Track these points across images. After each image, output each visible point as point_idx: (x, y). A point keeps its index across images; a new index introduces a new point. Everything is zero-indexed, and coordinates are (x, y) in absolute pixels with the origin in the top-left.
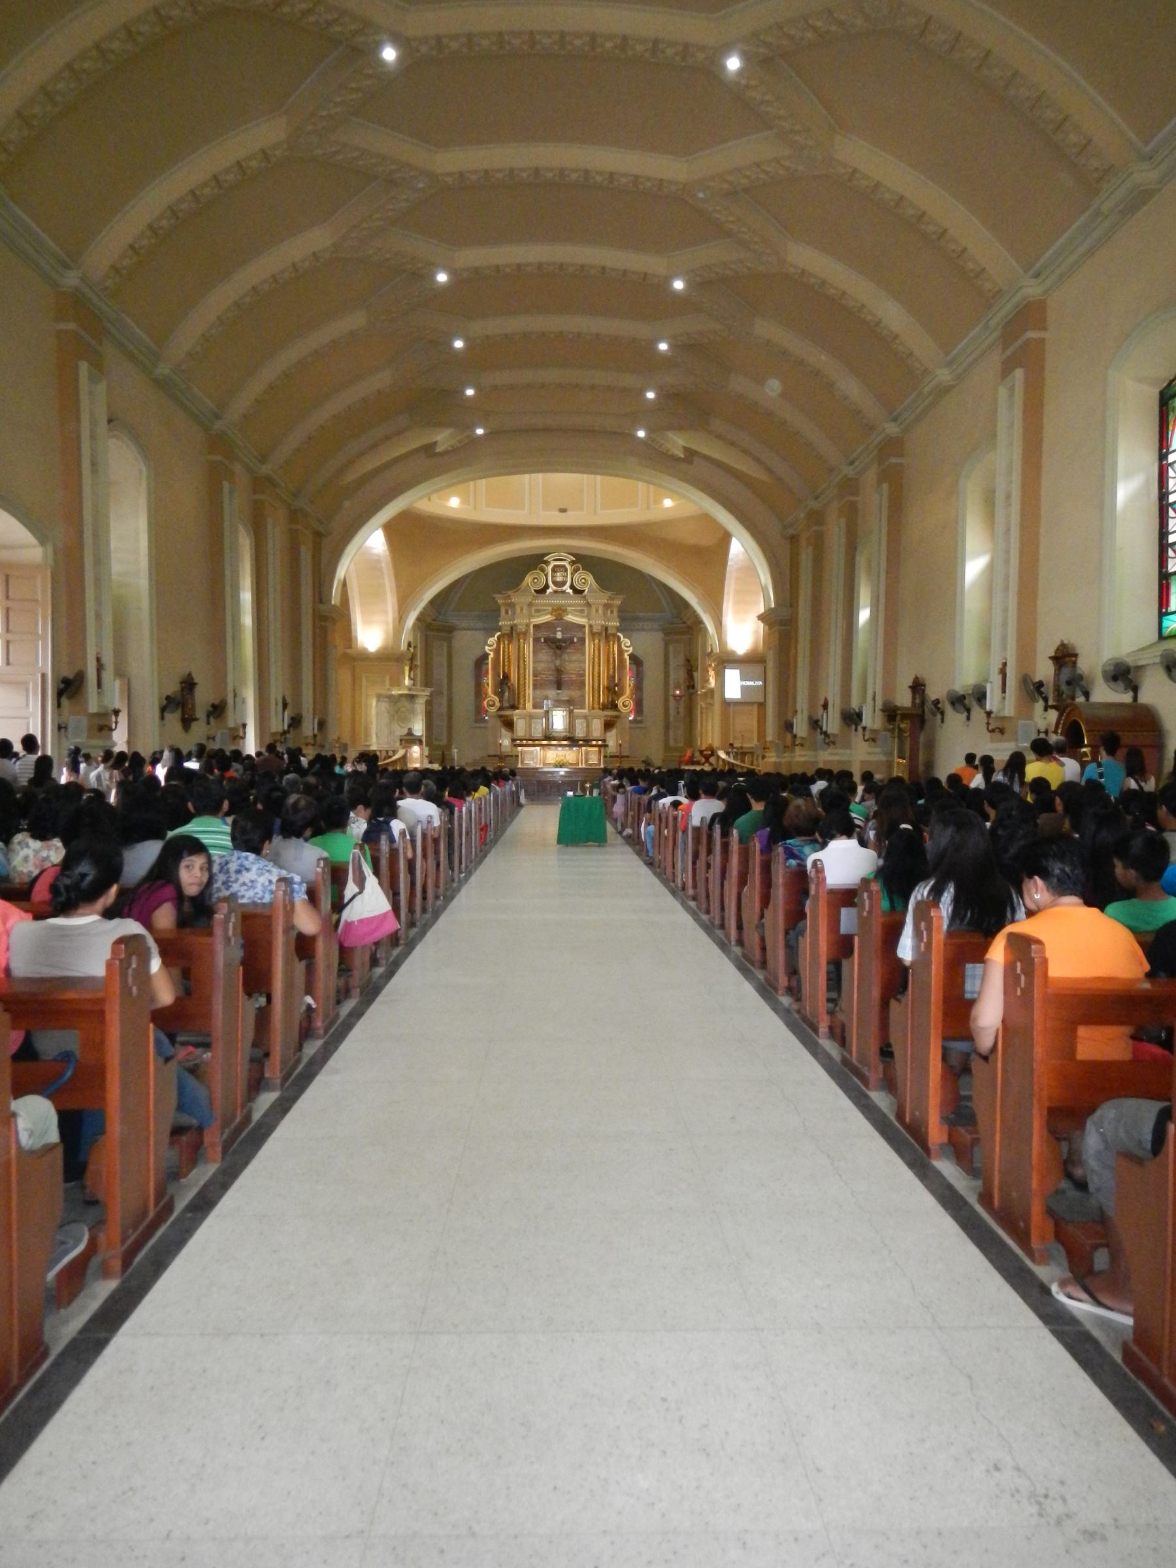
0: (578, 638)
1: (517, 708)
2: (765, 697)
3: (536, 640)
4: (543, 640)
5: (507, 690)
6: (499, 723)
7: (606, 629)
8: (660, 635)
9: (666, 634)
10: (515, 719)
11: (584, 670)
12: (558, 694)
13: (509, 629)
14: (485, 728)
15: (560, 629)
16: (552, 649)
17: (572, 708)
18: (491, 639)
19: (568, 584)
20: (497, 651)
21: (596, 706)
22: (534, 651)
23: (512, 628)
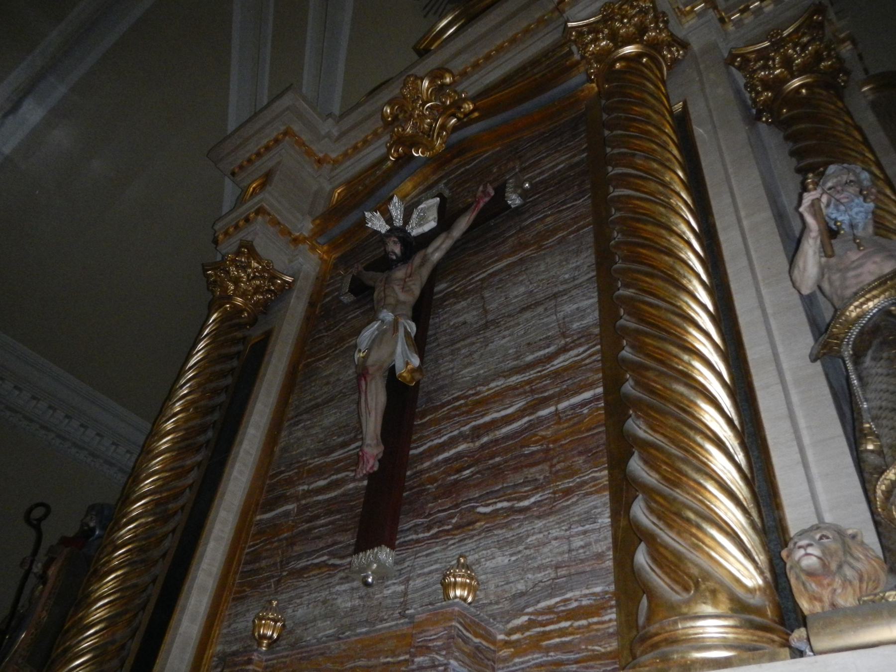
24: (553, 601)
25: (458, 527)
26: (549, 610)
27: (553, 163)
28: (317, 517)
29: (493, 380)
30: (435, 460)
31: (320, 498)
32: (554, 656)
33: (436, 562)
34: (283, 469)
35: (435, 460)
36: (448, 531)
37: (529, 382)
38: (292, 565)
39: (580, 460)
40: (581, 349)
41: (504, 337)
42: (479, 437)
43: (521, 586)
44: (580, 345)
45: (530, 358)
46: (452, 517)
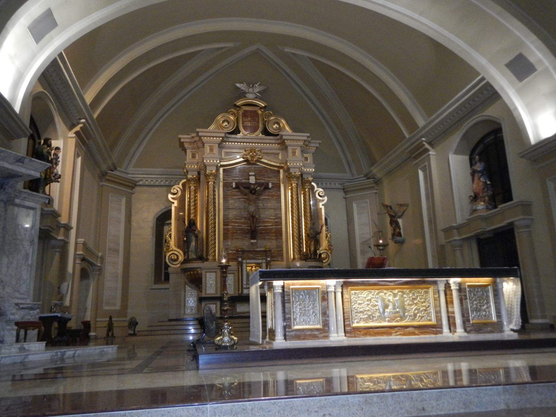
0: (272, 184)
1: (207, 260)
3: (226, 186)
4: (234, 186)
5: (193, 239)
6: (182, 279)
8: (341, 194)
10: (203, 272)
13: (196, 173)
14: (168, 289)
15: (253, 173)
16: (246, 195)
17: (269, 259)
20: (182, 200)
23: (199, 173)
25: (263, 239)
37: (272, 222)
38: (235, 237)
45: (272, 218)
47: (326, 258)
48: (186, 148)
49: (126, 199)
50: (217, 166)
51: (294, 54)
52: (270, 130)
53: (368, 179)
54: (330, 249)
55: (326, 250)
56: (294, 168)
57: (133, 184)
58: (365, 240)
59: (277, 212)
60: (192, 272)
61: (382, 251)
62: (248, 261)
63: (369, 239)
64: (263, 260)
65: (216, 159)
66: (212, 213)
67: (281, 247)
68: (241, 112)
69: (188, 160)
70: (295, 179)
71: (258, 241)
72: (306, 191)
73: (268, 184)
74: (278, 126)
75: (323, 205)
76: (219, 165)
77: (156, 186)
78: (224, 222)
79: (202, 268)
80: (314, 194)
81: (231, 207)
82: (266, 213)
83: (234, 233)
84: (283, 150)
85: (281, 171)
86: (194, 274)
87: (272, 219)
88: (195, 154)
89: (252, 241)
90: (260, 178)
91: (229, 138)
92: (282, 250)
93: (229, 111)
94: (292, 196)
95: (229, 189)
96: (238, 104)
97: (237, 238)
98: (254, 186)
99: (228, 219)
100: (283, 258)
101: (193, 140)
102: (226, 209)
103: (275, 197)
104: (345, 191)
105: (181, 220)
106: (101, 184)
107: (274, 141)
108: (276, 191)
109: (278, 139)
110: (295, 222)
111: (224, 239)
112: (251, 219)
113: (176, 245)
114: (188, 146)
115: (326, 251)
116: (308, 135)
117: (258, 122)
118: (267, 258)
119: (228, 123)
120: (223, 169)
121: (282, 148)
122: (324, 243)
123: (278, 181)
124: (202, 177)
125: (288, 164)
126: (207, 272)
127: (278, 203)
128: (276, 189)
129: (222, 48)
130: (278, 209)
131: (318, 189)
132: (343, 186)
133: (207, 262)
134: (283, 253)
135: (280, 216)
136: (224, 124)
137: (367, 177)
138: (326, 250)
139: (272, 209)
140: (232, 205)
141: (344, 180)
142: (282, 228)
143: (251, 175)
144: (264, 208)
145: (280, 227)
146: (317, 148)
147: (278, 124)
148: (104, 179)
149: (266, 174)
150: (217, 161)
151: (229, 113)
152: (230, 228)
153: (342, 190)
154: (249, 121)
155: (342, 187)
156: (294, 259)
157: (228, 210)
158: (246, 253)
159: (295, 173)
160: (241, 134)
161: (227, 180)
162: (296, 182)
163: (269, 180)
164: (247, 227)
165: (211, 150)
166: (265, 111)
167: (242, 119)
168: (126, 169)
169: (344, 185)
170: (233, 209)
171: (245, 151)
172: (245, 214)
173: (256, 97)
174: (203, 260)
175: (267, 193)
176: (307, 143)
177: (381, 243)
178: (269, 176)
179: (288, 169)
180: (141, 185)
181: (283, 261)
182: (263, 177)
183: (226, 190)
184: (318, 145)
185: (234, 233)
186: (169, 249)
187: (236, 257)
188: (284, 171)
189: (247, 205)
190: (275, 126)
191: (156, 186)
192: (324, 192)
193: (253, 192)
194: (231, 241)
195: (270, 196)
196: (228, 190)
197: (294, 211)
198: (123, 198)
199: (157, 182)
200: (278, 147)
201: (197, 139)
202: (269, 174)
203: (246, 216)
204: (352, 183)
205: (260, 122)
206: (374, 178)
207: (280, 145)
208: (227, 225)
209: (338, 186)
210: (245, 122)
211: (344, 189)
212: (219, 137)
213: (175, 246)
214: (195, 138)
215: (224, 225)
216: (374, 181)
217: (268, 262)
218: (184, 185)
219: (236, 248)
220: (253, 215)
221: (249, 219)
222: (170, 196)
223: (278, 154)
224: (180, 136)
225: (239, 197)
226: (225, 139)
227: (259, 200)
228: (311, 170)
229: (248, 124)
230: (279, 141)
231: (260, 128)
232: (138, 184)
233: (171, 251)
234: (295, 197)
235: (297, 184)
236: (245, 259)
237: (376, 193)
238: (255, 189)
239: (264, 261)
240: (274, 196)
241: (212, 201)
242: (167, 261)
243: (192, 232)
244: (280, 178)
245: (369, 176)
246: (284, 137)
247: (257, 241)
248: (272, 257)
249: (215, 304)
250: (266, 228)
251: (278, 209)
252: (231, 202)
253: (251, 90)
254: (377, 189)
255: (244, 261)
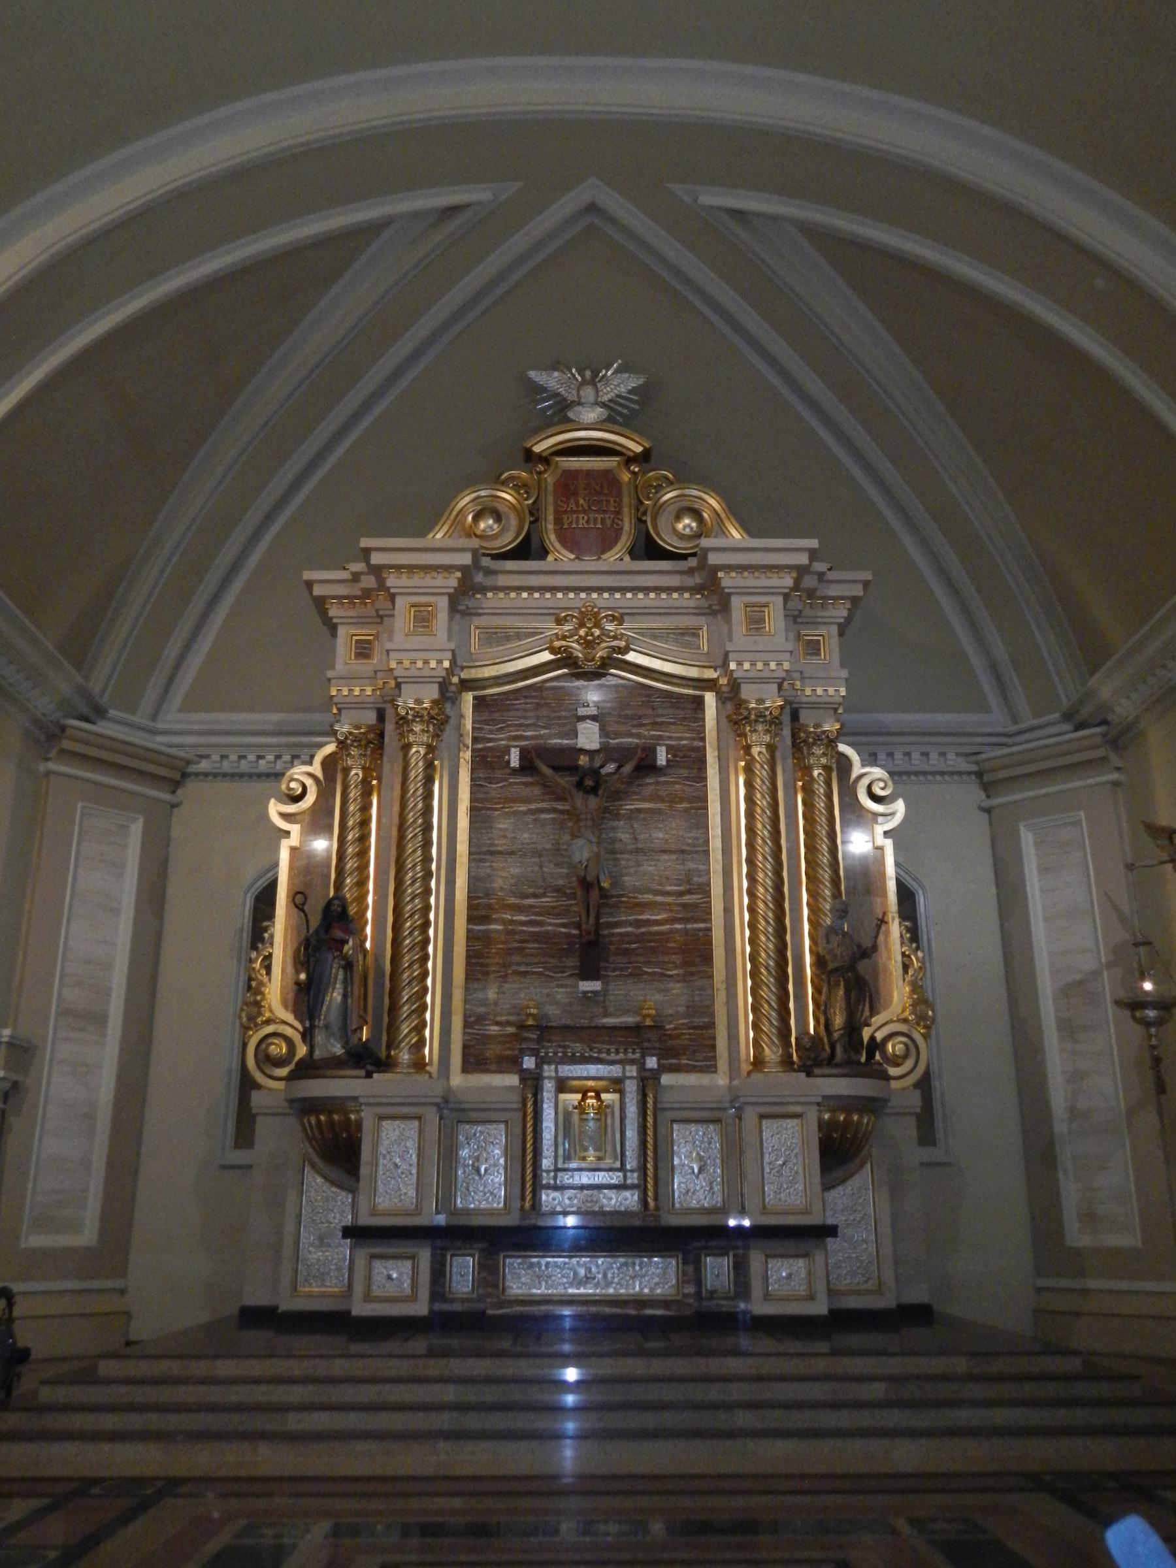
0: (669, 749)
1: (385, 1065)
2: (907, 1114)
4: (515, 761)
7: (795, 716)
8: (973, 794)
9: (988, 787)
10: (367, 1116)
11: (705, 889)
12: (588, 998)
13: (370, 717)
17: (652, 1062)
18: (299, 771)
19: (625, 541)
21: (771, 1054)
22: (474, 810)
23: (381, 716)
24: (685, 1021)
25: (631, 975)
26: (683, 1024)
27: (679, 735)
28: (527, 941)
29: (646, 893)
30: (612, 931)
31: (524, 928)
32: (686, 1042)
33: (621, 990)
34: (481, 895)
35: (612, 931)
36: (627, 976)
37: (669, 904)
38: (514, 967)
39: (698, 960)
40: (700, 896)
41: (651, 866)
42: (639, 927)
43: (670, 1011)
44: (698, 893)
45: (668, 888)
46: (629, 968)
47: (906, 1056)
48: (335, 621)
49: (146, 822)
50: (444, 686)
51: (739, 215)
52: (668, 542)
53: (1080, 726)
54: (921, 1018)
55: (905, 1021)
56: (752, 680)
57: (173, 768)
58: (1078, 977)
59: (692, 865)
60: (336, 1117)
61: (1153, 1030)
62: (566, 1070)
63: (1096, 974)
64: (628, 1067)
65: (439, 655)
66: (418, 868)
67: (708, 1011)
68: (550, 478)
69: (339, 668)
70: (760, 727)
71: (611, 987)
72: (811, 776)
73: (654, 752)
74: (694, 525)
75: (886, 834)
76: (455, 680)
77: (260, 776)
78: (471, 907)
79: (362, 1100)
80: (848, 792)
81: (501, 844)
82: (642, 868)
83: (509, 952)
84: (714, 613)
85: (710, 699)
86: (331, 1123)
87: (668, 894)
88: (369, 642)
89: (586, 986)
90: (622, 728)
91: (495, 572)
92: (712, 1025)
93: (503, 477)
94: (749, 799)
95: (498, 774)
96: (537, 449)
97: (525, 973)
98: (592, 759)
99: (487, 895)
100: (714, 1058)
101: (355, 590)
102: (477, 854)
103: (685, 805)
104: (986, 781)
105: (299, 900)
106: (42, 767)
107: (675, 581)
108: (687, 779)
109: (691, 571)
110: (761, 905)
111: (470, 977)
112: (579, 892)
113: (291, 997)
114: (341, 613)
115: (903, 1028)
116: (813, 543)
117: (618, 512)
118: (643, 1056)
119: (498, 518)
120: (475, 698)
121: (710, 606)
122: (895, 994)
123: (693, 739)
124: (389, 728)
125: (733, 666)
126: (382, 1118)
127: (698, 828)
128: (685, 773)
129: (451, 211)
130: (697, 852)
131: (867, 770)
132: (977, 763)
133: (387, 1076)
134: (714, 1038)
135: (701, 880)
136: (482, 525)
137: (1075, 718)
138: (905, 1021)
139: (672, 852)
140: (505, 837)
141: (979, 740)
142: (710, 929)
143: (582, 719)
144: (637, 851)
145: (702, 925)
146: (855, 600)
147: (696, 514)
148: (53, 754)
149: (649, 712)
150: (440, 662)
151: (504, 483)
152: (497, 931)
153: (973, 777)
154: (585, 512)
155: (974, 768)
156: (758, 1063)
157: (489, 857)
158: (553, 1038)
159: (760, 701)
160: (550, 558)
161: (490, 740)
162: (767, 738)
163: (660, 738)
164: (564, 925)
165: (423, 619)
166: (645, 473)
167: (556, 506)
168: (154, 717)
169: (983, 756)
170: (512, 853)
171: (559, 621)
172: (559, 875)
173: (610, 419)
174: (369, 1067)
175: (648, 790)
176: (809, 582)
177: (1147, 993)
178: (659, 720)
179: (735, 686)
180: (206, 775)
181: (712, 1069)
182: (634, 726)
183: (485, 779)
184: (858, 591)
185: (509, 952)
186: (260, 1014)
187: (516, 1052)
188: (722, 700)
189: (567, 838)
190: (687, 524)
191: (260, 776)
192: (890, 783)
193: (589, 782)
194: (496, 985)
195: (663, 801)
196: (490, 780)
197: (760, 858)
198: (135, 820)
199: (262, 762)
200: (692, 603)
201: (369, 582)
202: (660, 711)
203: (561, 882)
204: (1015, 749)
205: (626, 510)
206: (1105, 722)
207: (703, 595)
208: (485, 919)
209: (954, 762)
210: (565, 517)
211: (979, 775)
212: (449, 569)
213: (286, 1007)
214: (363, 577)
215: (471, 919)
216: (1104, 735)
217: (647, 1074)
218: (328, 763)
219: (519, 1014)
220: (585, 878)
221: (573, 896)
222: (275, 809)
223: (694, 632)
224: (307, 575)
225: (533, 807)
226: (479, 578)
227: (617, 816)
228: (831, 691)
229: (577, 523)
230: (697, 579)
231: (624, 538)
232: (192, 768)
233: (268, 1022)
234: (762, 801)
235: (771, 748)
236: (549, 1063)
237: (1116, 784)
238: (595, 773)
239: (632, 1071)
240: (681, 800)
241: (420, 821)
242: (251, 1063)
243: (330, 949)
244: (704, 726)
245: (1085, 712)
246: (713, 559)
247: (605, 985)
248: (665, 1053)
249: (412, 1257)
250: (644, 930)
251: (697, 852)
252: (503, 824)
253: (588, 393)
254: (1118, 769)
255: (549, 1070)
